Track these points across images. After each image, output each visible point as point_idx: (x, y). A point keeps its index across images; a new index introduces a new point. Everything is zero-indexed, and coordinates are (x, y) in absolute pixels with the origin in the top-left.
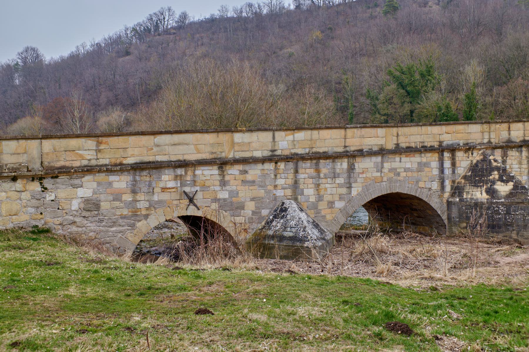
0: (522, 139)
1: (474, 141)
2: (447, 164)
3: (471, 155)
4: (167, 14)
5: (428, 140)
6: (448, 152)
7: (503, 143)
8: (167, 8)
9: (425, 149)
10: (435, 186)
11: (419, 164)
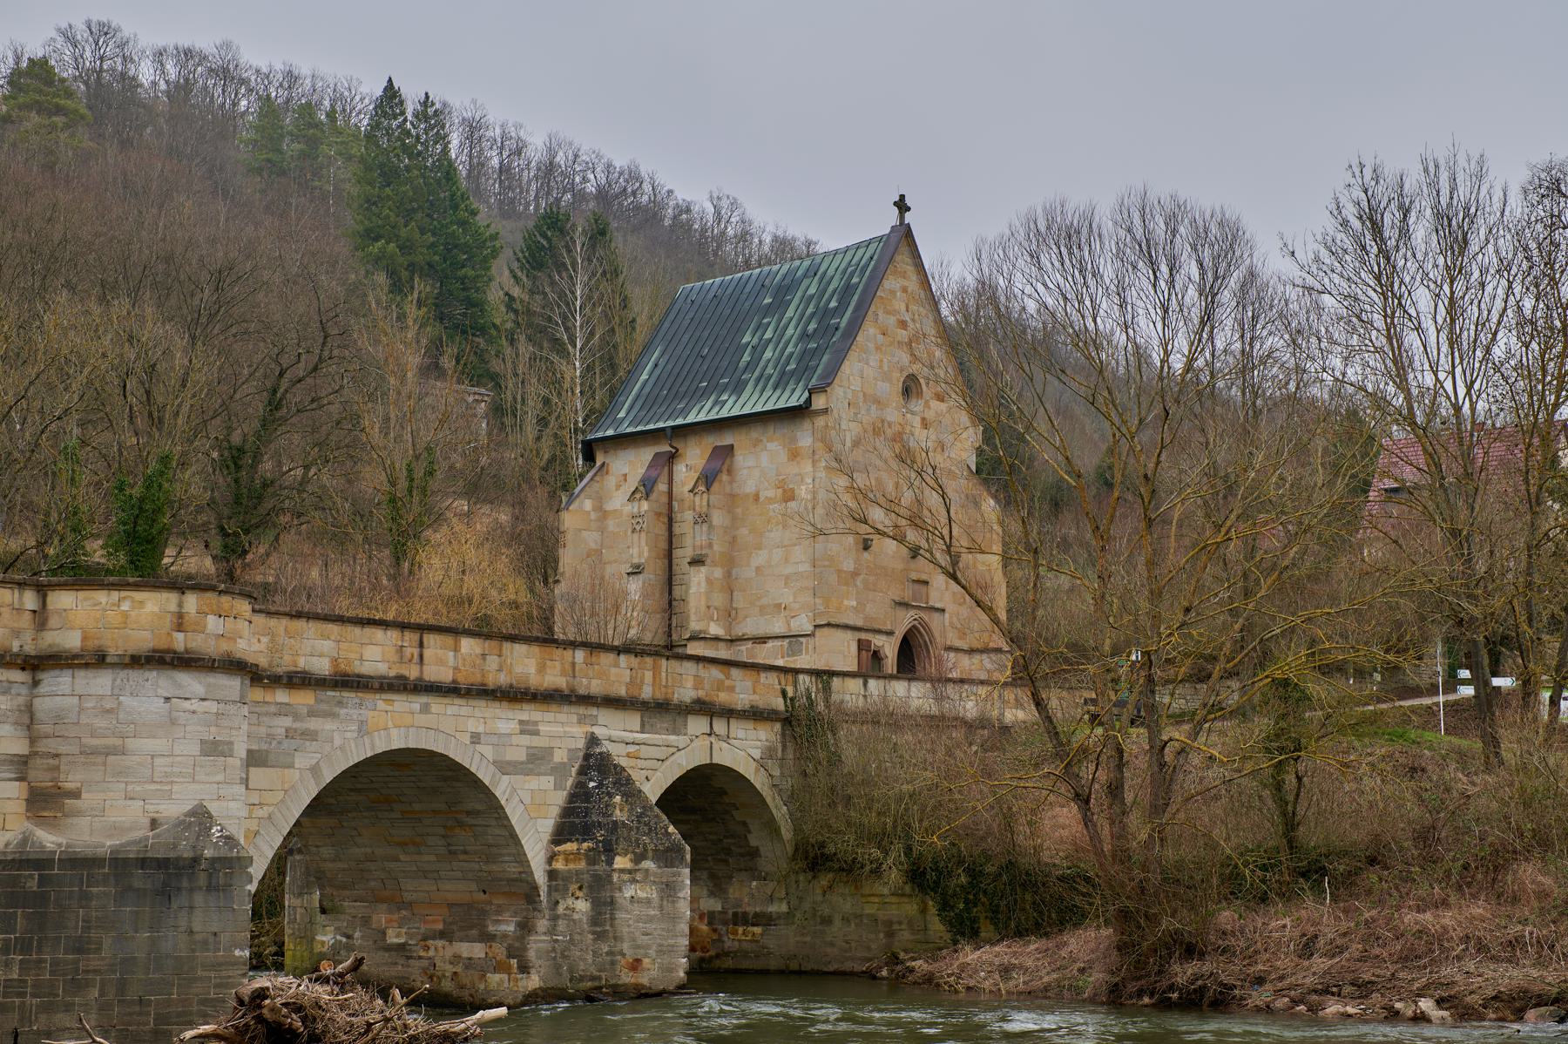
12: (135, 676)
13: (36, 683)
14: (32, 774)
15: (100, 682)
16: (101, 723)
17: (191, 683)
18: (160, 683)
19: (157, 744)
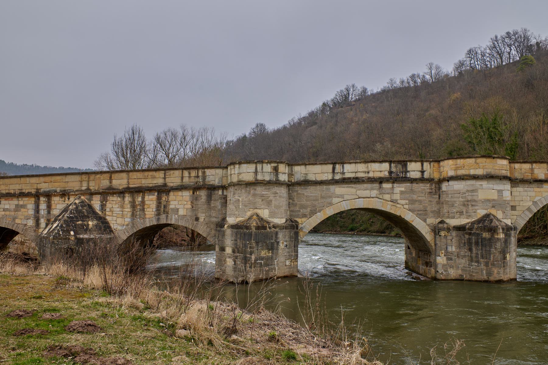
0: (126, 186)
1: (72, 188)
2: (43, 206)
4: (352, 90)
5: (26, 188)
6: (44, 197)
7: (103, 190)
8: (351, 85)
9: (22, 195)
10: (31, 223)
11: (17, 206)
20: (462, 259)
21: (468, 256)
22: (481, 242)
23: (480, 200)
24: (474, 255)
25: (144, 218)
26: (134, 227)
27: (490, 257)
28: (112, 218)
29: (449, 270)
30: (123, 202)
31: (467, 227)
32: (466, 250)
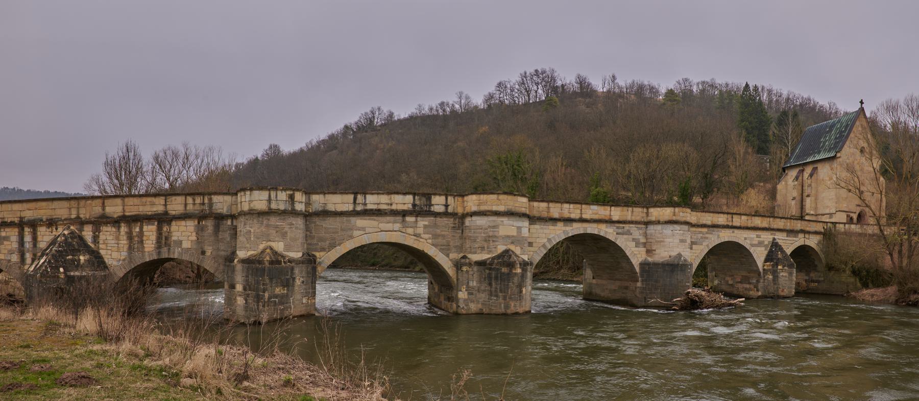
0: (122, 214)
3: (54, 230)
4: (377, 113)
8: (377, 108)
12: (666, 226)
13: (647, 228)
14: (647, 246)
15: (659, 227)
16: (659, 236)
17: (677, 227)
18: (670, 227)
19: (670, 240)
20: (482, 293)
21: (488, 290)
22: (501, 277)
23: (501, 237)
24: (493, 289)
25: (143, 252)
26: (132, 262)
27: (508, 291)
28: (107, 252)
29: (470, 304)
30: (118, 233)
31: (488, 262)
32: (486, 285)
